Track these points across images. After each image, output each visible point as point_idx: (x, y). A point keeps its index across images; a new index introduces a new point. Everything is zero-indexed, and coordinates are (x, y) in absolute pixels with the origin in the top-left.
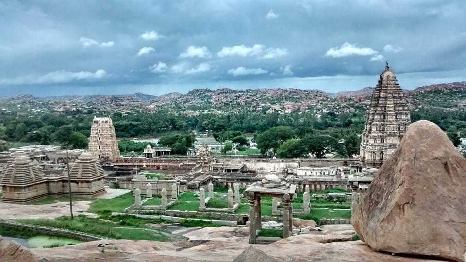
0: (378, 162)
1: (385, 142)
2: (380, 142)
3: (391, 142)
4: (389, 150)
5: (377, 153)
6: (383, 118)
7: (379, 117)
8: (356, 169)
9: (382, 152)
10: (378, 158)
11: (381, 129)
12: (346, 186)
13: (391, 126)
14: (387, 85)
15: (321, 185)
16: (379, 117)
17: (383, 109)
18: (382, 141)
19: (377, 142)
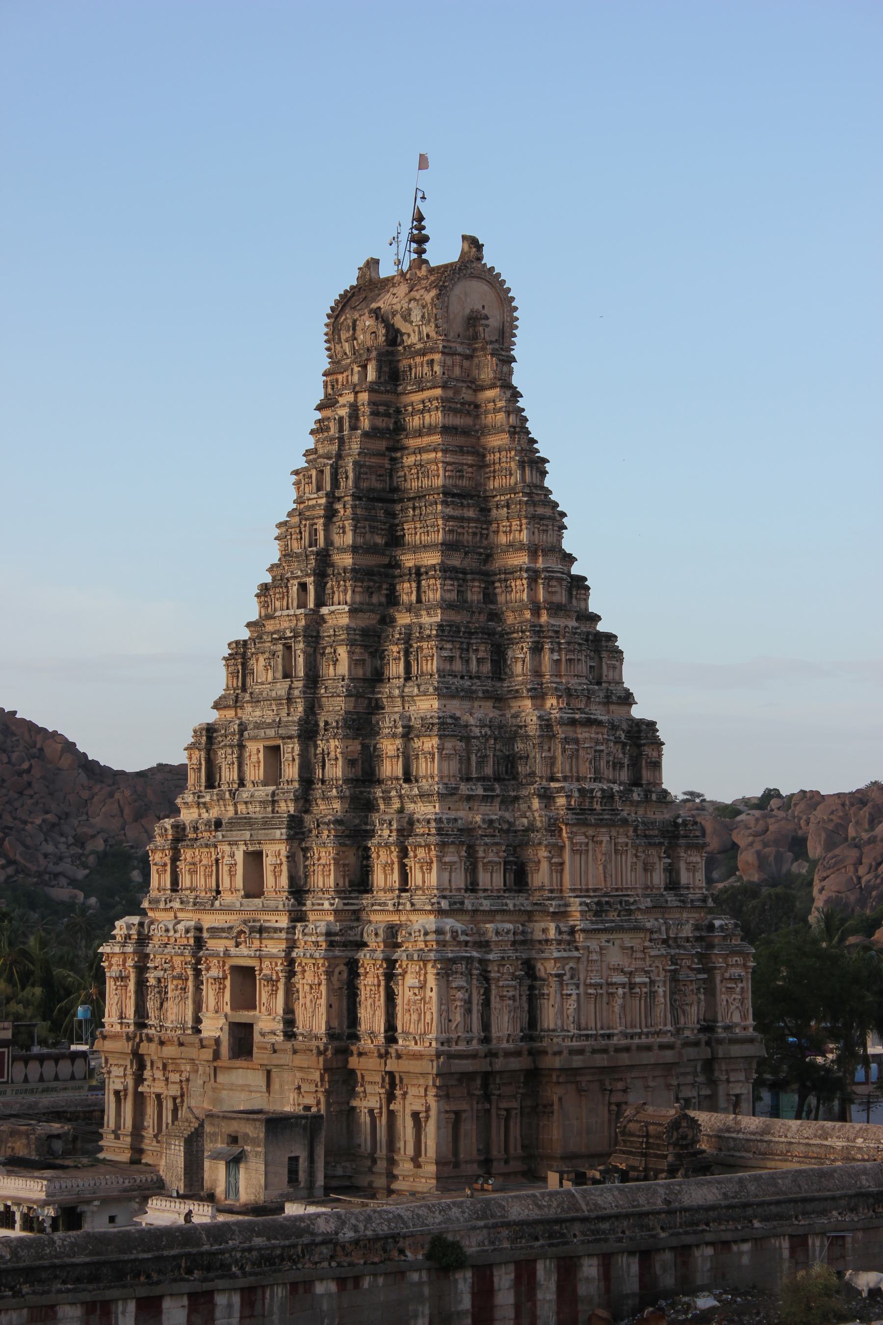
0: (515, 1064)
1: (541, 877)
2: (498, 880)
3: (595, 878)
4: (594, 945)
5: (505, 981)
6: (487, 668)
7: (458, 666)
8: (303, 1155)
9: (529, 967)
10: (505, 1025)
11: (489, 770)
12: (786, 1244)
13: (582, 733)
14: (466, 395)
15: (606, 1261)
16: (458, 666)
17: (474, 595)
18: (518, 876)
19: (484, 879)
